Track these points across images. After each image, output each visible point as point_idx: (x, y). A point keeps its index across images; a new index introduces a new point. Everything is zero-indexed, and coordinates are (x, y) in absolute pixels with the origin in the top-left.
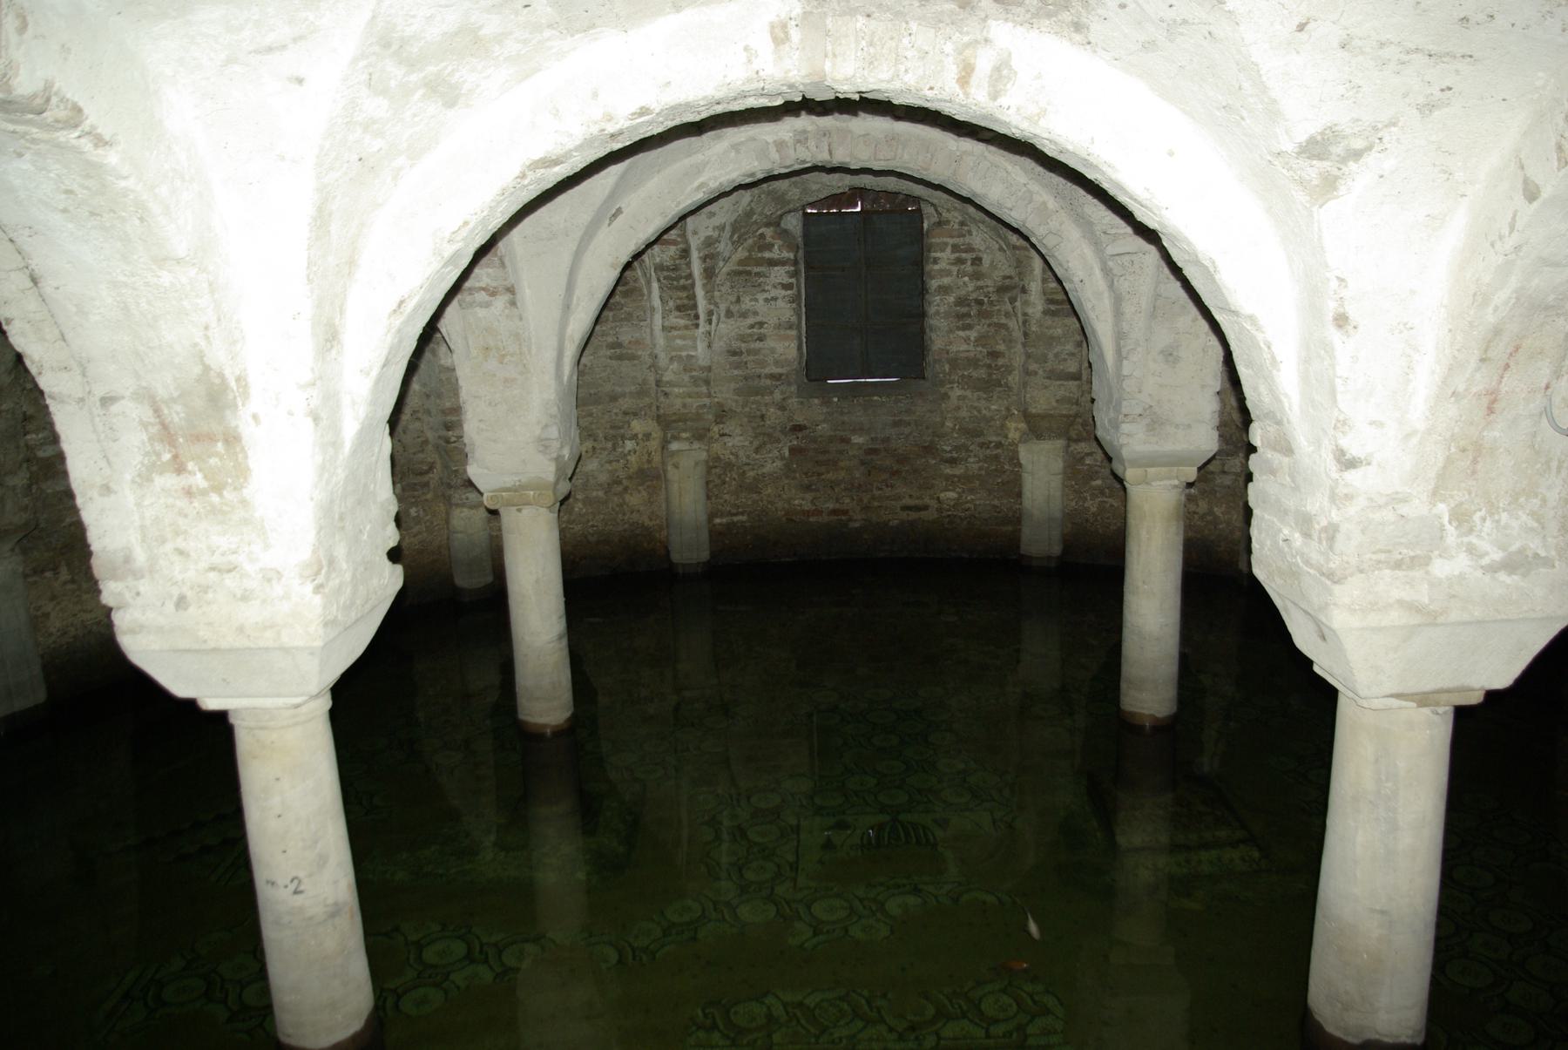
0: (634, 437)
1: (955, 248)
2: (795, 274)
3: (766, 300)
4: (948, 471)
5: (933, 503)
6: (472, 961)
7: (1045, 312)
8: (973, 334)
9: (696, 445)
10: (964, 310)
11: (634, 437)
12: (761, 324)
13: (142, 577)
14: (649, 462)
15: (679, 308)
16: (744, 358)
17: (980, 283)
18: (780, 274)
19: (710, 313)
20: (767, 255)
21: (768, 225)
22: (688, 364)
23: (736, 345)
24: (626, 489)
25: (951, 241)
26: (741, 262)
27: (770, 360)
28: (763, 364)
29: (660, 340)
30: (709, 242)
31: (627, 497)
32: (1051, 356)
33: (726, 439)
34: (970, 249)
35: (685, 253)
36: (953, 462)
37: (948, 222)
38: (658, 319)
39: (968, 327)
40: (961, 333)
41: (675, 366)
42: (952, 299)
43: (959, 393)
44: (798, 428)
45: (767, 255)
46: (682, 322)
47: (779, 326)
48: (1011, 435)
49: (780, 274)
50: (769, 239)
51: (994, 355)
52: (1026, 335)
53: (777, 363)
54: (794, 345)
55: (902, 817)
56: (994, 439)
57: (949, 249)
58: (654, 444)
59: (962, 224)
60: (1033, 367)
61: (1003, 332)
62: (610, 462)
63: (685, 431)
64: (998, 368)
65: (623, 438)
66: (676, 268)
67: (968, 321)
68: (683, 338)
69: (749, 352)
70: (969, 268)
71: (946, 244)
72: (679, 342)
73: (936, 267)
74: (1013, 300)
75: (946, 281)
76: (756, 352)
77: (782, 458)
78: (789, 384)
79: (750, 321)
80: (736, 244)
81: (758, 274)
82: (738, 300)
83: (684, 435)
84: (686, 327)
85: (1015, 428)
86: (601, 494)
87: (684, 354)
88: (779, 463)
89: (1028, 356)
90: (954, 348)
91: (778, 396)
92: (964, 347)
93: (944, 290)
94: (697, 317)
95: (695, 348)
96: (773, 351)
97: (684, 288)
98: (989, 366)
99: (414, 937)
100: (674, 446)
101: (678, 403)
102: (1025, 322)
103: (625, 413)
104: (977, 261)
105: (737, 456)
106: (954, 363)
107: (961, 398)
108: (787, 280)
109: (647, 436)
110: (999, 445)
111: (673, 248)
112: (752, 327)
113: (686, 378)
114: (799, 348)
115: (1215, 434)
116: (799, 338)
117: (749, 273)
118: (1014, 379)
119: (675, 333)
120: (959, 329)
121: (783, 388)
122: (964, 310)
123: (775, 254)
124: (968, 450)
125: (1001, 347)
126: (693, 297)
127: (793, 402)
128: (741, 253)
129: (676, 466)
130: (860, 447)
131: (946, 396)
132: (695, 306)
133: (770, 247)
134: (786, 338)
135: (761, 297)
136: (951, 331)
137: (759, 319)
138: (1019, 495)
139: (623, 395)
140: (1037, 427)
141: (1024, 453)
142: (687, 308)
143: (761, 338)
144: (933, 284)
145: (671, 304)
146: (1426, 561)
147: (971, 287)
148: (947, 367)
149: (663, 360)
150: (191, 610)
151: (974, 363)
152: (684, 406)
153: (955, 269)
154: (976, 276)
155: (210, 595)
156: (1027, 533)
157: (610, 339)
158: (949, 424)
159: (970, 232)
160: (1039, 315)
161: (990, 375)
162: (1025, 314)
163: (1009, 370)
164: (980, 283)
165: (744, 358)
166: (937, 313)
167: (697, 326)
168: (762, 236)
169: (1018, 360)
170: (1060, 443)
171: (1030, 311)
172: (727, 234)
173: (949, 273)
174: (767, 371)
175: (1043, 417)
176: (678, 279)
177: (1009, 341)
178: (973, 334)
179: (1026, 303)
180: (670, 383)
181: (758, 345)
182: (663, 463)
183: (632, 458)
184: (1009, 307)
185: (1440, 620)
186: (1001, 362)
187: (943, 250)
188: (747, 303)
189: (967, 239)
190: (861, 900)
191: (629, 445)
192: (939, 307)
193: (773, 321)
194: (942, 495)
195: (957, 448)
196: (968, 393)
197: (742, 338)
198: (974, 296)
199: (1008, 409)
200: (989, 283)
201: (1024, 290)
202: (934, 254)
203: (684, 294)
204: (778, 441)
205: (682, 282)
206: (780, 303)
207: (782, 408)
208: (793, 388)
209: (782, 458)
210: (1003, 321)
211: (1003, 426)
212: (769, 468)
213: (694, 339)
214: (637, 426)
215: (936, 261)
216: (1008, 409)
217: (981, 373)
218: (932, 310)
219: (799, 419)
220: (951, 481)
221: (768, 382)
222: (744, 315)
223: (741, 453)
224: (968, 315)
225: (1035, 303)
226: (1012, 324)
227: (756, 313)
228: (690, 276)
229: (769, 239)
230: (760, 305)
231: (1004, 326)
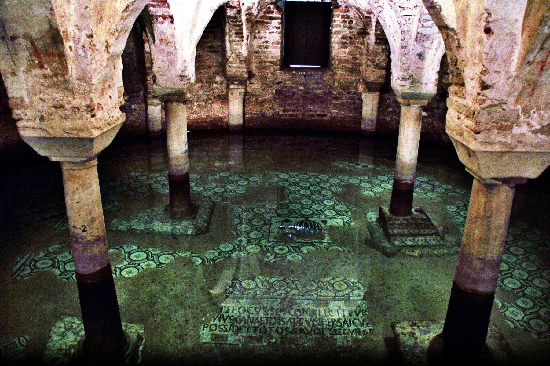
0: (217, 83)
1: (343, 17)
2: (280, 24)
3: (270, 33)
4: (335, 102)
5: (329, 115)
6: (148, 260)
7: (376, 43)
8: (347, 50)
9: (240, 87)
10: (345, 41)
11: (217, 83)
12: (267, 42)
13: (28, 108)
14: (222, 92)
15: (236, 34)
16: (260, 54)
17: (352, 31)
18: (276, 23)
19: (248, 36)
20: (271, 15)
21: (272, 4)
22: (239, 55)
23: (257, 49)
24: (213, 102)
25: (341, 14)
26: (261, 18)
27: (270, 55)
28: (266, 57)
29: (228, 45)
30: (249, 9)
31: (213, 105)
32: (376, 60)
33: (251, 85)
34: (348, 17)
35: (239, 12)
36: (337, 99)
37: (341, 6)
38: (227, 38)
39: (346, 47)
40: (343, 50)
41: (233, 56)
42: (340, 36)
43: (341, 72)
44: (281, 82)
45: (271, 15)
46: (237, 39)
47: (274, 43)
48: (359, 89)
49: (276, 23)
50: (272, 9)
51: (355, 59)
52: (368, 51)
53: (272, 57)
54: (279, 51)
55: (309, 219)
56: (353, 90)
57: (340, 17)
58: (224, 86)
59: (346, 7)
60: (369, 63)
61: (359, 50)
62: (207, 91)
63: (236, 81)
64: (356, 64)
65: (213, 83)
66: (236, 18)
67: (346, 45)
68: (237, 45)
69: (262, 52)
70: (348, 25)
71: (339, 15)
72: (235, 46)
73: (335, 24)
74: (363, 38)
75: (338, 29)
76: (265, 52)
77: (272, 93)
78: (277, 65)
79: (263, 40)
80: (259, 11)
81: (267, 23)
82: (259, 32)
83: (236, 83)
84: (239, 41)
85: (361, 88)
86: (204, 104)
87: (237, 51)
88: (271, 95)
89: (368, 60)
90: (340, 56)
91: (272, 70)
92: (344, 55)
93: (338, 33)
94: (243, 37)
95: (242, 49)
96: (271, 52)
97: (238, 26)
98: (353, 63)
99: (127, 250)
100: (232, 87)
101: (234, 70)
102: (368, 46)
103: (214, 73)
104: (351, 22)
105: (255, 92)
106: (340, 60)
107: (341, 74)
108: (278, 25)
109: (222, 83)
110: (355, 93)
111: (235, 10)
112: (263, 43)
113: (238, 61)
114: (281, 52)
115: (436, 88)
116: (281, 48)
117: (263, 22)
118: (362, 69)
119: (234, 43)
120: (342, 48)
121: (275, 67)
122: (345, 41)
123: (274, 15)
124: (343, 95)
125: (358, 56)
126: (241, 29)
127: (278, 72)
128: (261, 14)
129: (232, 94)
130: (301, 90)
131: (335, 74)
132: (242, 33)
133: (272, 12)
134: (276, 48)
135: (268, 31)
136: (339, 48)
137: (266, 40)
138: (361, 112)
139: (214, 66)
140: (370, 87)
141: (363, 96)
142: (239, 34)
143: (267, 47)
144: (334, 30)
145: (233, 32)
146: (511, 128)
147: (348, 32)
148: (337, 62)
149: (229, 53)
150: (46, 122)
151: (346, 61)
152: (236, 71)
153: (342, 25)
154: (350, 28)
155: (53, 117)
156: (362, 126)
157: (209, 45)
158: (336, 84)
159: (348, 11)
160: (373, 44)
161: (353, 66)
162: (368, 43)
163: (360, 65)
164: (352, 31)
165: (260, 54)
166: (335, 41)
167: (243, 41)
168: (269, 8)
169: (364, 61)
170: (378, 93)
171: (369, 42)
172: (256, 5)
173: (340, 26)
174: (268, 60)
175: (372, 83)
176: (236, 22)
177: (361, 54)
178: (347, 50)
179: (369, 39)
180: (232, 63)
181: (266, 50)
182: (227, 93)
183: (216, 91)
184: (361, 40)
185: (515, 150)
186: (357, 61)
187: (338, 17)
188: (262, 34)
189: (348, 14)
190: (292, 247)
191: (215, 85)
192: (335, 39)
193: (272, 41)
194: (332, 111)
195: (339, 94)
196: (344, 73)
197: (260, 47)
198: (349, 35)
199: (359, 80)
200: (355, 31)
201: (369, 34)
202: (334, 19)
203: (238, 28)
204: (271, 87)
205: (238, 23)
206: (275, 34)
207: (273, 74)
208: (278, 67)
209: (272, 93)
210: (359, 46)
211: (357, 86)
212: (267, 97)
213: (242, 46)
214: (218, 79)
215: (335, 21)
216: (359, 80)
217: (350, 66)
218: (333, 40)
219: (280, 79)
220: (336, 106)
221: (269, 64)
222: (261, 38)
223: (257, 90)
224: (346, 43)
225: (372, 39)
226: (362, 47)
227: (265, 38)
228: (241, 21)
229: (272, 9)
230: (267, 35)
231: (360, 48)
